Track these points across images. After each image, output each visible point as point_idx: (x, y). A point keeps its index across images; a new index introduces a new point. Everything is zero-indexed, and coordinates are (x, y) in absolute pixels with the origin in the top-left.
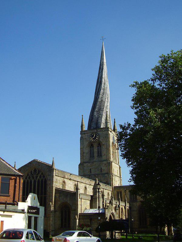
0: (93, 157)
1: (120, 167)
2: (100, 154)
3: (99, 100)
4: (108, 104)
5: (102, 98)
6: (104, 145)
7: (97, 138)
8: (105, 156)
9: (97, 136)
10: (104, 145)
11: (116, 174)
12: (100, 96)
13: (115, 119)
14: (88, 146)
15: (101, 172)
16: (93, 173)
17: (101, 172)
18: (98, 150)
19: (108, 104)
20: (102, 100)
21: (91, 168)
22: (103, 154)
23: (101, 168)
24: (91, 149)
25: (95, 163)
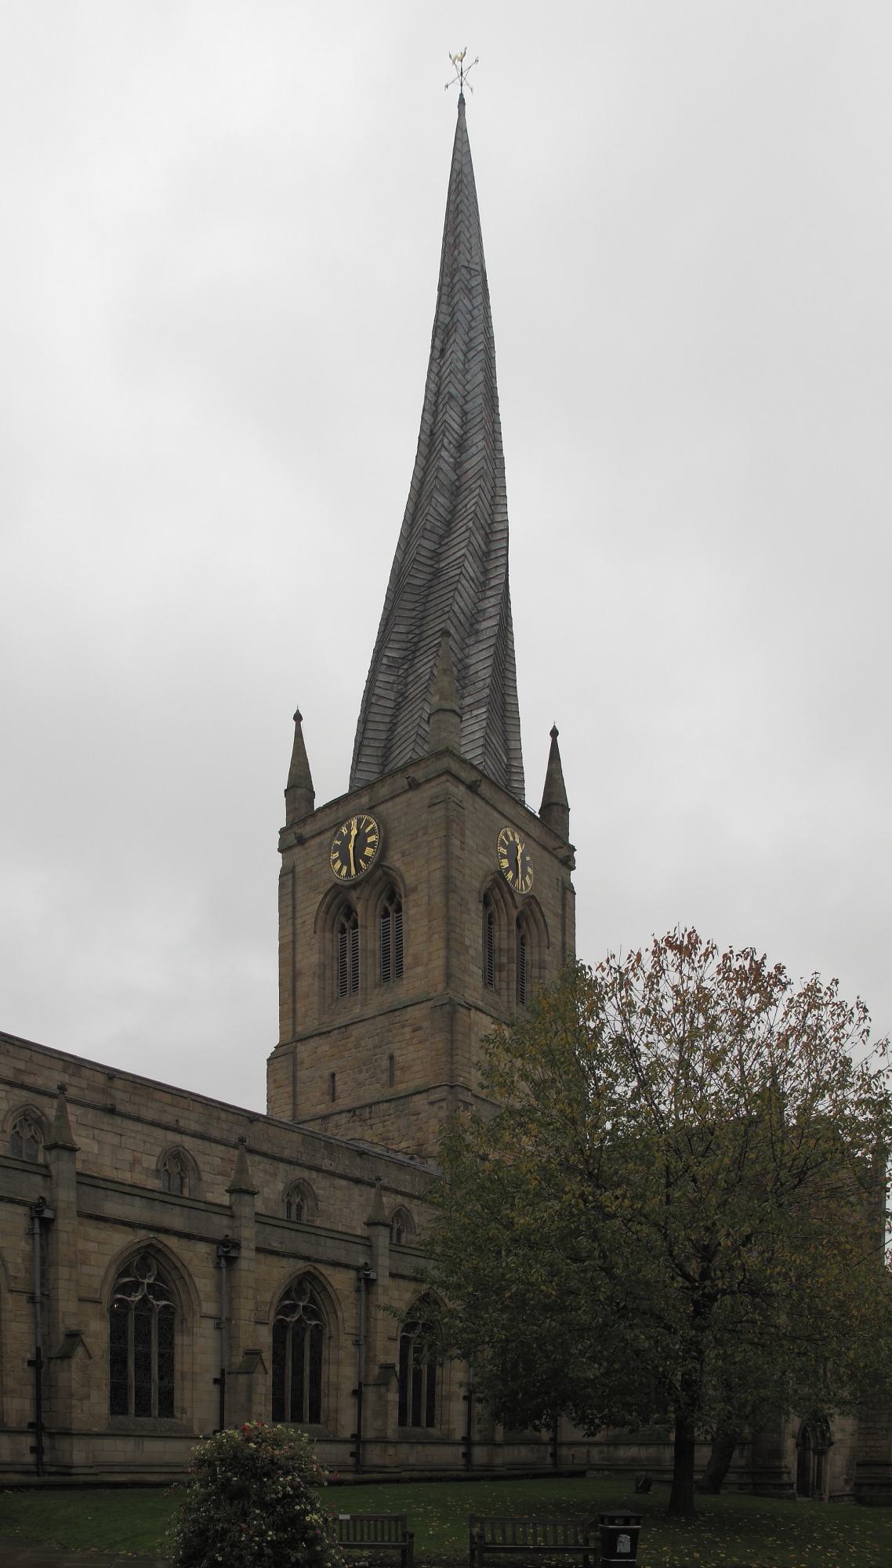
7: (369, 852)
8: (420, 969)
9: (372, 832)
14: (320, 923)
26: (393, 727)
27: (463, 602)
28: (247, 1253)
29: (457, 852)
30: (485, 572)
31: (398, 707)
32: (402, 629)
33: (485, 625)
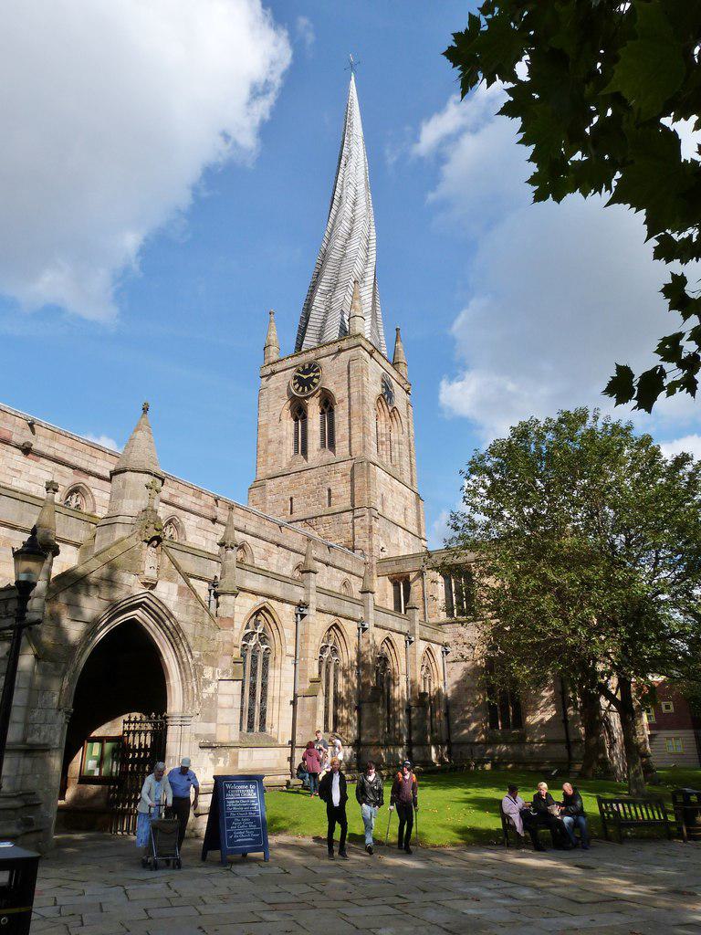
0: (305, 452)
1: (418, 497)
2: (329, 441)
3: (335, 256)
4: (370, 270)
5: (344, 247)
6: (342, 401)
7: (315, 380)
10: (342, 401)
11: (399, 519)
12: (339, 242)
13: (397, 330)
15: (330, 505)
16: (296, 516)
17: (330, 505)
18: (323, 423)
19: (366, 270)
20: (344, 255)
21: (291, 493)
22: (337, 438)
23: (329, 490)
24: (297, 425)
25: (307, 474)
26: (324, 321)
27: (358, 267)
28: (311, 611)
29: (366, 384)
30: (367, 256)
31: (327, 312)
32: (327, 277)
33: (367, 279)
